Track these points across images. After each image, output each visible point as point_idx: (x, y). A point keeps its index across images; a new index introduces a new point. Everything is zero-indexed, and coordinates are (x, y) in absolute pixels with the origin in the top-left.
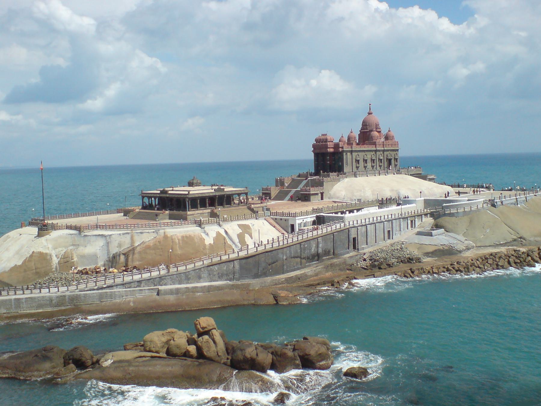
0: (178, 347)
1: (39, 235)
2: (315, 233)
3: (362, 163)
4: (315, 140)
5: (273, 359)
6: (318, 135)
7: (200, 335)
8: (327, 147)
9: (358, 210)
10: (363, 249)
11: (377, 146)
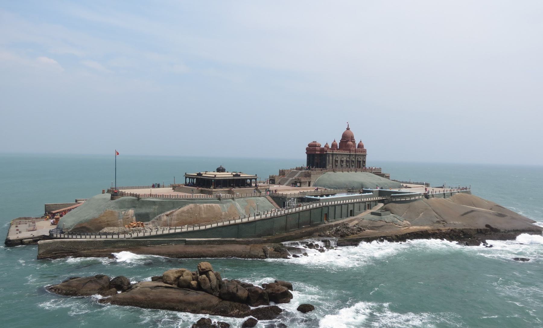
0: (185, 281)
1: (112, 199)
2: (297, 209)
3: (339, 162)
4: (309, 145)
5: (248, 294)
6: (310, 142)
7: (201, 274)
9: (332, 195)
10: (332, 221)
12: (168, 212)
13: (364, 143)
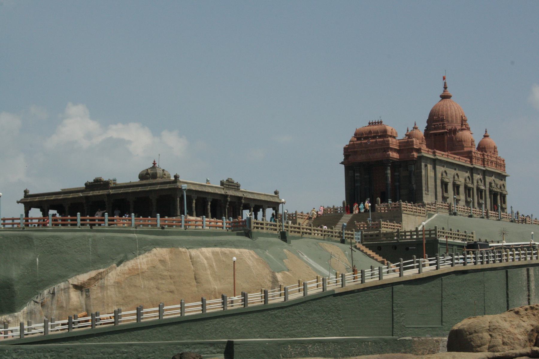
8: (386, 148)
11: (474, 160)
12: (83, 278)
13: (492, 141)
